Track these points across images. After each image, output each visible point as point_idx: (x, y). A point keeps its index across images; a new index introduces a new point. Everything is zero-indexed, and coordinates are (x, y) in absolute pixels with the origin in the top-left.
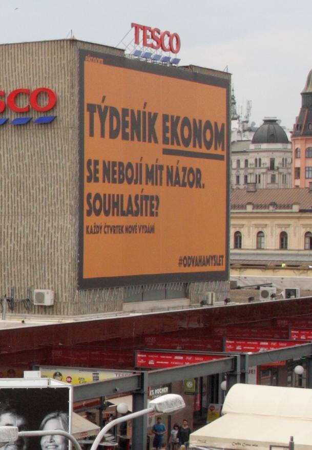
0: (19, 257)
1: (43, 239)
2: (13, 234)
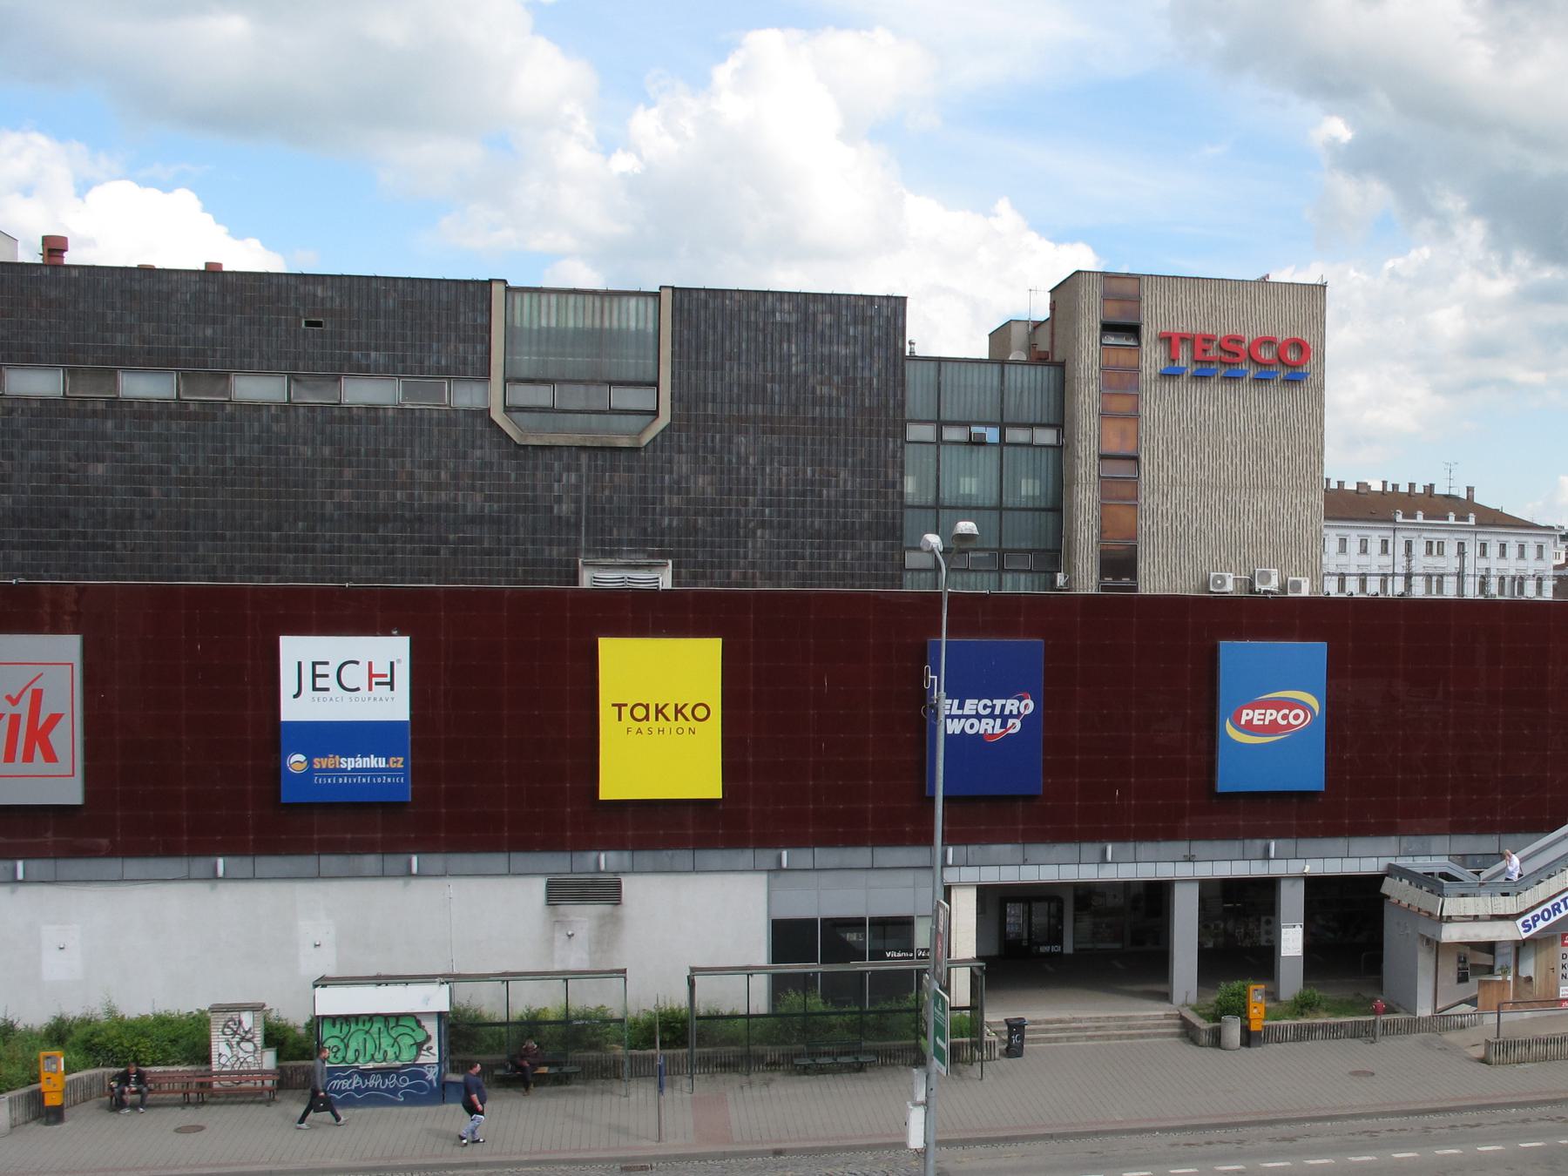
0: (1258, 539)
1: (1289, 517)
2: (1251, 510)
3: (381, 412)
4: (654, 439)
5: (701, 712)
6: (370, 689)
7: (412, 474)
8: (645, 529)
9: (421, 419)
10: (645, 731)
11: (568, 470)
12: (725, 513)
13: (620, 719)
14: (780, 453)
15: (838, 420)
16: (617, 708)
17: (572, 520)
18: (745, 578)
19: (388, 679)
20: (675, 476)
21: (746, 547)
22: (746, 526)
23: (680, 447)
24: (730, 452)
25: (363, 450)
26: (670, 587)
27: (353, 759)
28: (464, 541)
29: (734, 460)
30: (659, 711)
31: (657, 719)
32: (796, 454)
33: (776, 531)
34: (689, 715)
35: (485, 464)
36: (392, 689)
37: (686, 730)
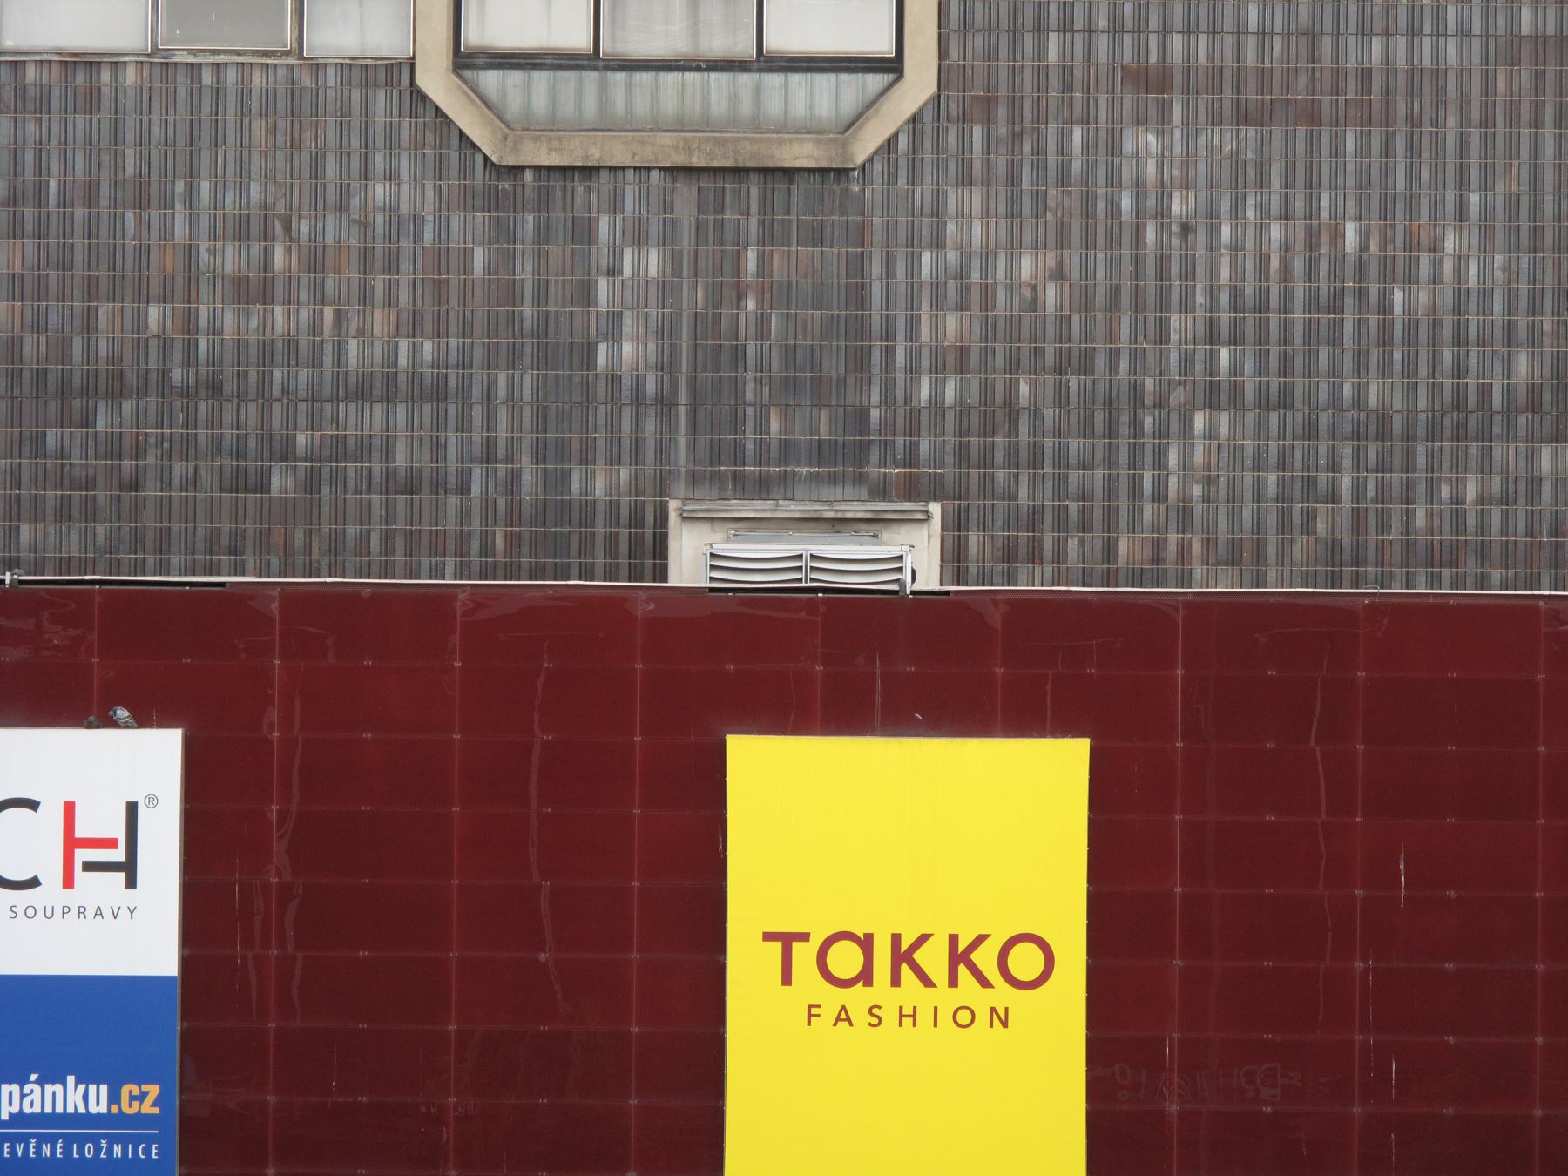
3: (106, 76)
4: (890, 144)
5: (1026, 962)
6: (68, 882)
7: (190, 251)
8: (862, 415)
9: (218, 92)
10: (860, 1016)
11: (640, 238)
12: (1100, 362)
13: (787, 979)
14: (1262, 183)
15: (1438, 74)
16: (777, 946)
17: (651, 387)
18: (1157, 559)
19: (119, 855)
20: (951, 255)
21: (1160, 463)
22: (1161, 404)
23: (965, 164)
24: (1113, 180)
25: (53, 185)
26: (934, 585)
27: (15, 1088)
28: (338, 449)
29: (1126, 203)
30: (902, 957)
31: (896, 981)
32: (1312, 185)
33: (1249, 416)
34: (992, 973)
35: (404, 224)
36: (131, 883)
37: (983, 1016)
